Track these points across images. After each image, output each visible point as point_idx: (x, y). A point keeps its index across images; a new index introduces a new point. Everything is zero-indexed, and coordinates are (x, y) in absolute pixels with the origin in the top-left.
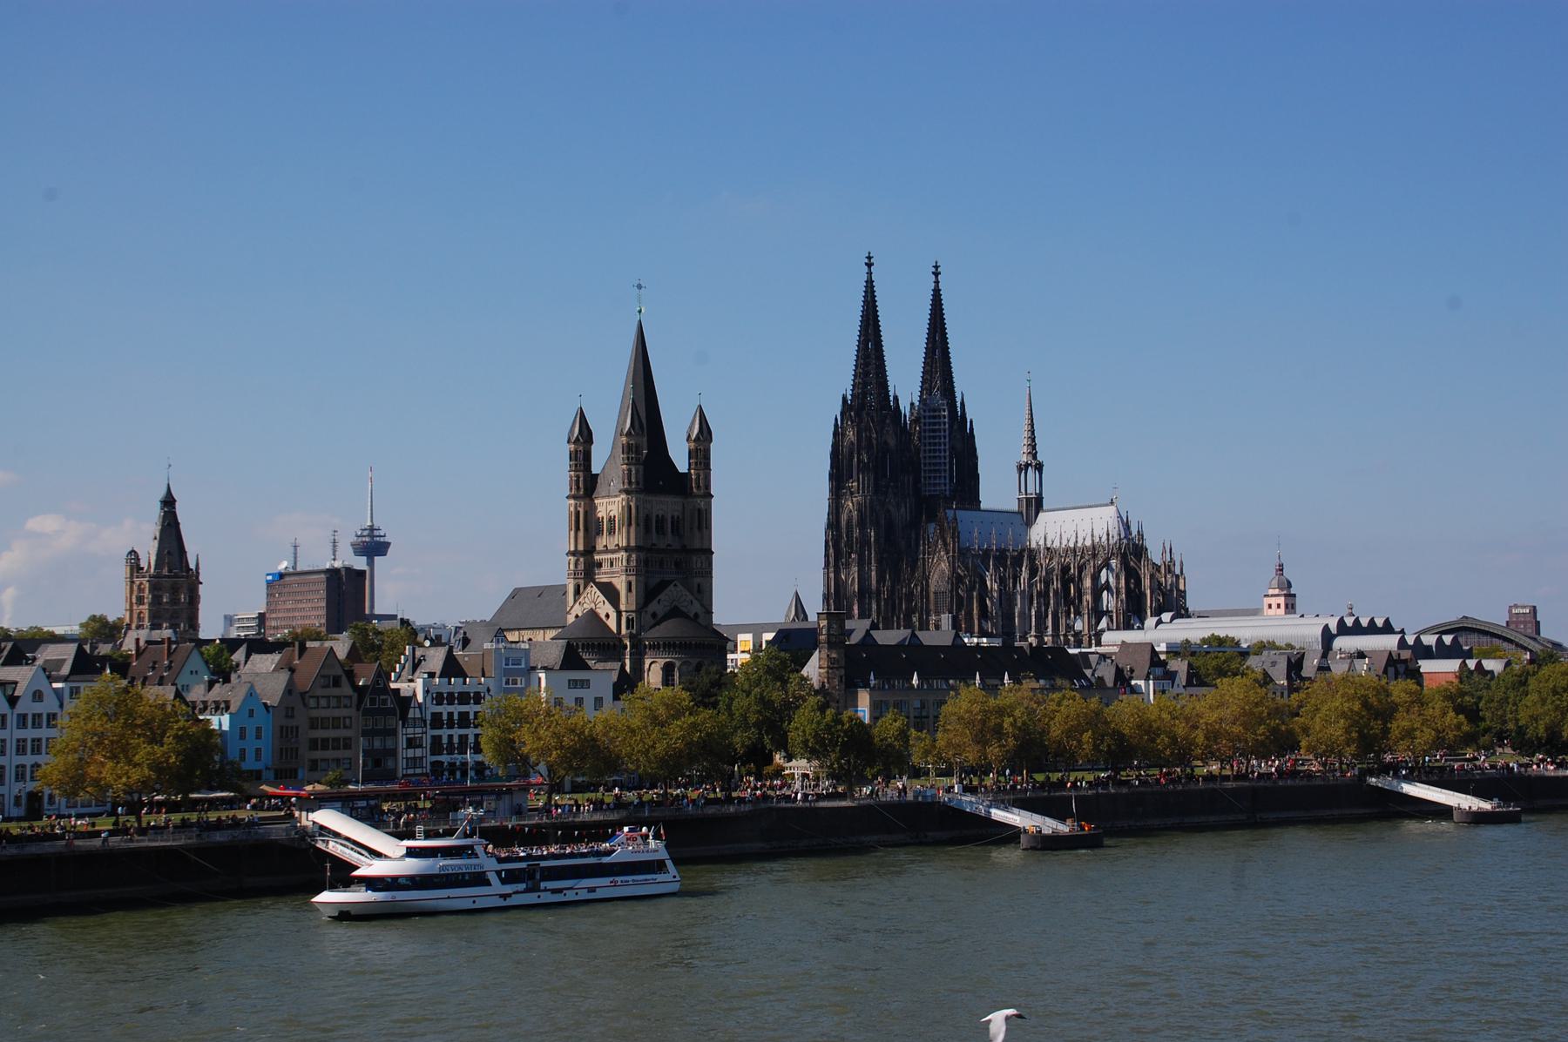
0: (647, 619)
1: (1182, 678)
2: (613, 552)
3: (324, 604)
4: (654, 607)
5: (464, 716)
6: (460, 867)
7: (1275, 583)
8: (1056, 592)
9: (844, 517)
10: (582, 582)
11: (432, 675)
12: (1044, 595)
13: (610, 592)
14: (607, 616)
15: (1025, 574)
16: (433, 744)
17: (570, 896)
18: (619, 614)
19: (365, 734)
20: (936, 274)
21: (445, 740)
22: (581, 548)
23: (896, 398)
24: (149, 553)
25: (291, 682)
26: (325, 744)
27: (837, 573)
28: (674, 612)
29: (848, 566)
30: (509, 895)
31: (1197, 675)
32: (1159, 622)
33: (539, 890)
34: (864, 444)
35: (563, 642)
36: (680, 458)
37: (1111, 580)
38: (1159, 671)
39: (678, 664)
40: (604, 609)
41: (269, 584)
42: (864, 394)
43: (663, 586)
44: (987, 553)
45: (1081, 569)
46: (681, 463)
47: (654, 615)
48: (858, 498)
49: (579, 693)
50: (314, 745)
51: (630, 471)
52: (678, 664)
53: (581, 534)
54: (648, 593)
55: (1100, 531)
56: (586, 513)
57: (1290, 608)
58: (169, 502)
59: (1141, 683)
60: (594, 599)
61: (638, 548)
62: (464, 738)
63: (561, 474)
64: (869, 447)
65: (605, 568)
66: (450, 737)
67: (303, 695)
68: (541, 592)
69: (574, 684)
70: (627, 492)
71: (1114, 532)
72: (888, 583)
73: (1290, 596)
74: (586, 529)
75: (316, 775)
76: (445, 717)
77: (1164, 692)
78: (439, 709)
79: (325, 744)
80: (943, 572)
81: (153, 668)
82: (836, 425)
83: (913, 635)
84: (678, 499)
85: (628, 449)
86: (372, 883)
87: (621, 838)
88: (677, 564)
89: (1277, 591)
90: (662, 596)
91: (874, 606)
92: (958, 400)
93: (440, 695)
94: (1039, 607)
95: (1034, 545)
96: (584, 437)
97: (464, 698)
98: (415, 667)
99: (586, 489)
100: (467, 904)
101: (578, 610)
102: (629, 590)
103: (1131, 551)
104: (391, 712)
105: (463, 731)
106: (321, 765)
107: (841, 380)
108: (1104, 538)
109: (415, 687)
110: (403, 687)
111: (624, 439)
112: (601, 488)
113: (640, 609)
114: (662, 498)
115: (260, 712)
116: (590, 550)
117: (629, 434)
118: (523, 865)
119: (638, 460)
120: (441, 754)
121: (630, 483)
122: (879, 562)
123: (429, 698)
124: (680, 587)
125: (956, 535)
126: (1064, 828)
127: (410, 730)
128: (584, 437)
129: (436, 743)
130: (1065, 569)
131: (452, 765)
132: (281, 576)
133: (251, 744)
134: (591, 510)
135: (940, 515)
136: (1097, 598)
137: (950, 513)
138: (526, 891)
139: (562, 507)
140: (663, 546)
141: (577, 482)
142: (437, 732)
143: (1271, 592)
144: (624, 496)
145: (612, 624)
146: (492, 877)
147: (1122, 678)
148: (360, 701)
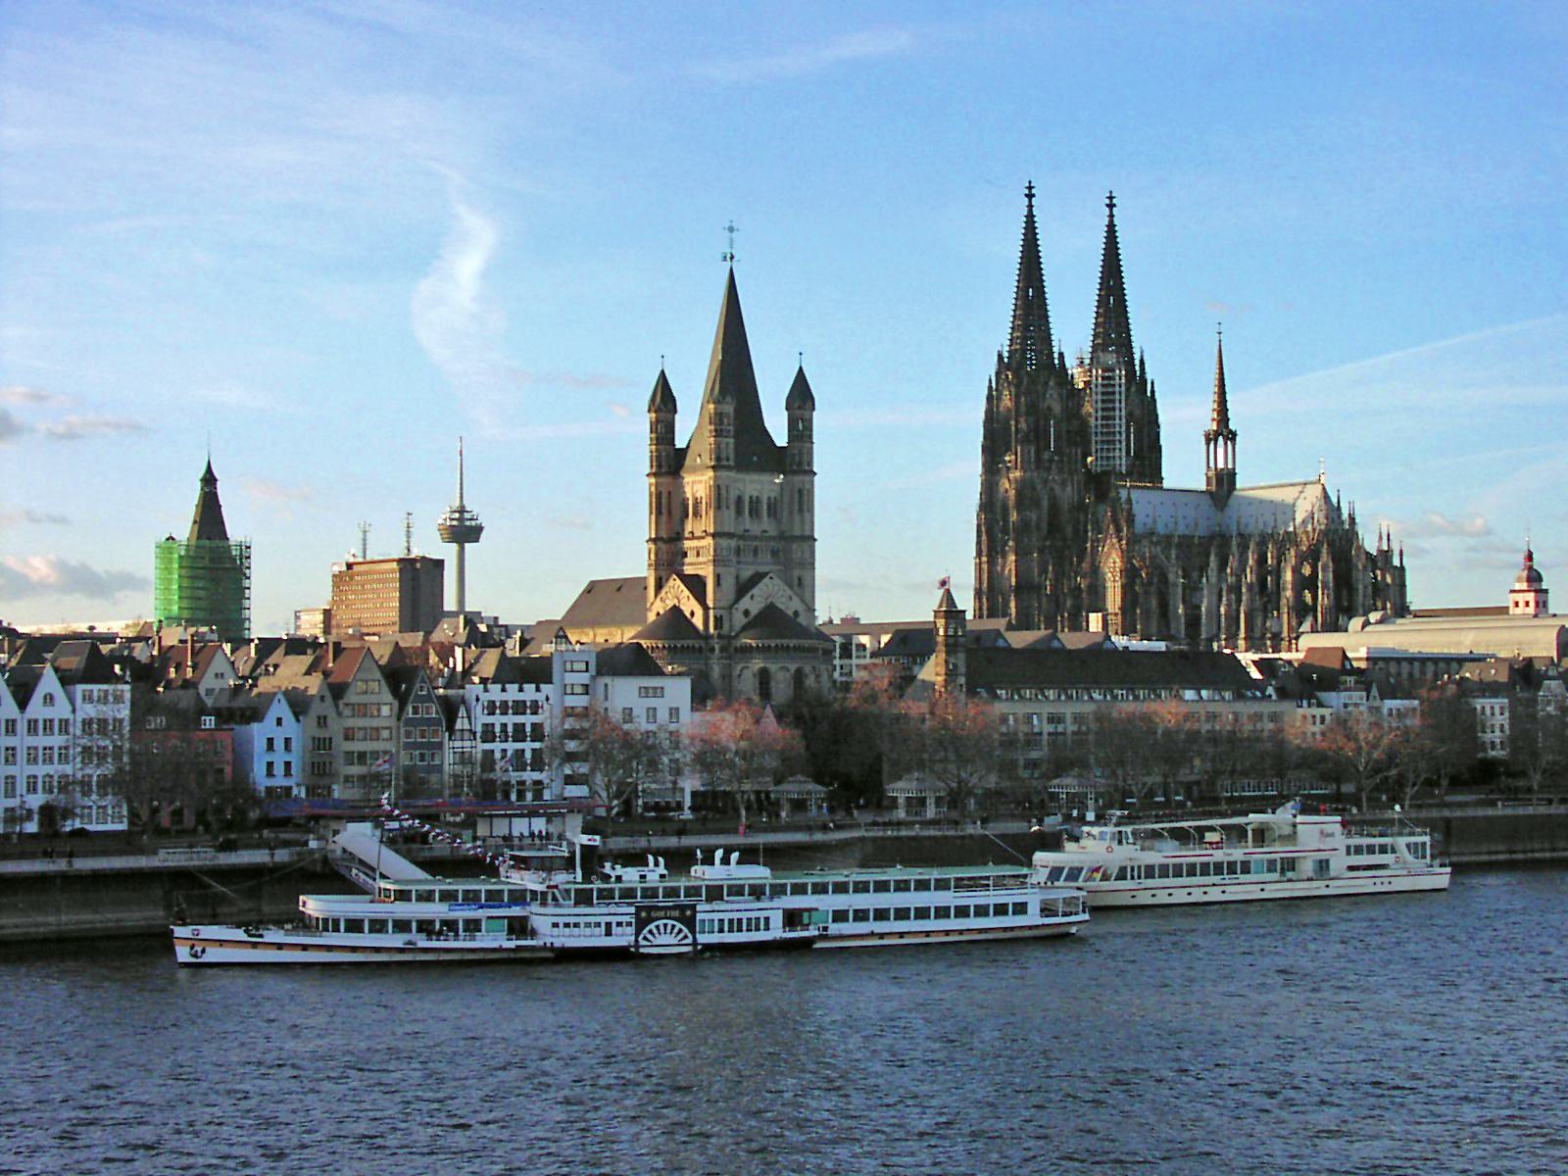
4: (745, 603)
5: (519, 728)
8: (1250, 587)
12: (1236, 589)
13: (696, 585)
14: (692, 614)
18: (706, 608)
23: (1061, 355)
27: (991, 563)
29: (1004, 556)
32: (1366, 623)
36: (777, 426)
40: (690, 605)
43: (757, 578)
46: (781, 439)
47: (746, 613)
49: (652, 702)
58: (209, 480)
60: (678, 594)
65: (687, 560)
68: (620, 585)
69: (645, 692)
74: (670, 513)
76: (497, 729)
78: (490, 719)
82: (990, 387)
88: (774, 553)
90: (755, 591)
92: (1137, 357)
94: (1229, 605)
96: (664, 401)
97: (520, 708)
99: (669, 466)
105: (519, 745)
107: (997, 333)
114: (755, 477)
124: (777, 581)
125: (1131, 520)
127: (458, 744)
133: (279, 757)
137: (1124, 494)
139: (639, 486)
142: (488, 746)
143: (1517, 586)
145: (698, 621)
148: (402, 709)
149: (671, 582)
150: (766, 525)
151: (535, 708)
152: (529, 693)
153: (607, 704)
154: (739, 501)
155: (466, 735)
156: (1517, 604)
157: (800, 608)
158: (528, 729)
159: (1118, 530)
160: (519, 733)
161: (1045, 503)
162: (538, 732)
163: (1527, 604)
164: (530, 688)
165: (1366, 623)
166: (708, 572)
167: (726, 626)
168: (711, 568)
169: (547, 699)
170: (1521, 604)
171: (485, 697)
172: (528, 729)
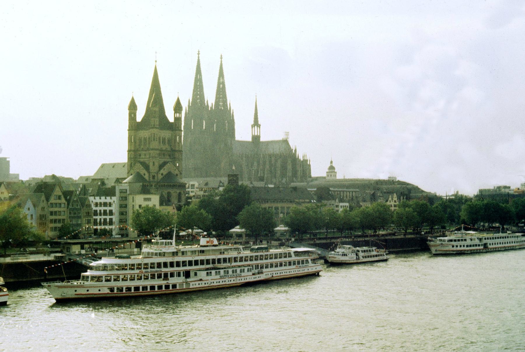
4: (162, 171)
5: (105, 211)
14: (145, 174)
16: (94, 223)
21: (98, 221)
43: (165, 163)
46: (171, 119)
47: (162, 174)
62: (105, 220)
66: (100, 219)
69: (145, 199)
76: (98, 212)
84: (171, 132)
88: (169, 156)
90: (165, 167)
97: (105, 204)
128: (133, 107)
140: (164, 149)
145: (146, 177)
148: (68, 204)
150: (166, 147)
151: (110, 205)
152: (108, 200)
153: (134, 203)
154: (159, 138)
157: (178, 173)
158: (108, 212)
160: (105, 213)
162: (111, 213)
164: (108, 198)
167: (156, 178)
171: (95, 201)
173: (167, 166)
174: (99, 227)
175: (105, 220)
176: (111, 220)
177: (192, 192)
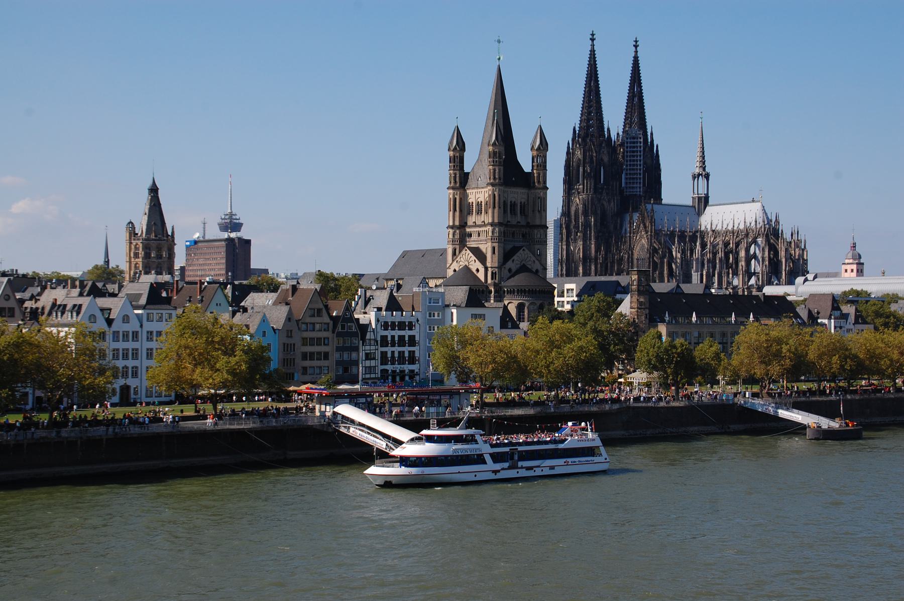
0: (505, 273)
1: (852, 318)
2: (480, 226)
3: (224, 261)
4: (509, 264)
5: (402, 338)
6: (466, 450)
7: (850, 255)
8: (721, 260)
9: (573, 209)
10: (457, 247)
11: (379, 309)
12: (712, 262)
13: (479, 254)
14: (478, 270)
15: (698, 247)
17: (538, 472)
18: (486, 269)
19: (339, 349)
20: (636, 46)
21: (389, 355)
22: (457, 223)
23: (608, 129)
24: (141, 225)
25: (290, 312)
26: (311, 356)
27: (568, 245)
28: (523, 269)
29: (575, 240)
30: (498, 471)
31: (861, 316)
32: (806, 280)
33: (517, 468)
34: (587, 160)
35: (467, 288)
37: (757, 252)
38: (837, 313)
39: (527, 304)
41: (187, 247)
42: (588, 127)
44: (672, 234)
45: (737, 244)
46: (527, 168)
47: (510, 270)
48: (583, 196)
50: (305, 356)
51: (495, 170)
52: (527, 304)
53: (457, 214)
54: (506, 256)
55: (750, 219)
56: (461, 199)
57: (860, 272)
58: (154, 190)
59: (826, 321)
60: (467, 258)
61: (500, 224)
62: (401, 354)
63: (444, 172)
64: (591, 162)
65: (473, 238)
66: (393, 352)
67: (298, 321)
68: (424, 253)
69: (475, 316)
70: (493, 185)
71: (760, 220)
72: (603, 253)
73: (860, 264)
74: (461, 211)
75: (307, 378)
76: (389, 339)
77: (841, 328)
78: (385, 333)
79: (311, 356)
80: (643, 245)
81: (190, 301)
82: (568, 147)
83: (678, 286)
85: (493, 155)
86: (404, 461)
87: (568, 431)
88: (523, 236)
89: (851, 261)
90: (515, 257)
91: (593, 267)
93: (386, 323)
94: (708, 269)
95: (703, 228)
97: (402, 326)
98: (367, 302)
99: (461, 183)
100: (470, 478)
101: (455, 266)
102: (494, 253)
103: (772, 233)
104: (354, 335)
106: (309, 371)
108: (753, 224)
109: (369, 317)
110: (363, 319)
111: (491, 148)
112: (471, 181)
113: (501, 267)
115: (270, 333)
116: (463, 225)
117: (494, 144)
118: (507, 449)
119: (500, 162)
120: (386, 364)
121: (495, 178)
122: (597, 238)
123: (379, 326)
125: (653, 221)
126: (835, 424)
127: (368, 348)
128: (460, 146)
129: (384, 359)
130: (726, 244)
131: (394, 372)
132: (196, 242)
134: (464, 197)
135: (643, 207)
136: (748, 264)
138: (510, 468)
139: (444, 195)
140: (514, 223)
141: (455, 177)
142: (384, 349)
143: (847, 261)
144: (490, 188)
146: (488, 458)
147: (813, 318)
148: (335, 327)
149: (464, 252)
151: (411, 326)
155: (372, 342)
156: (846, 271)
158: (407, 339)
159: (645, 227)
160: (401, 341)
161: (599, 212)
162: (412, 341)
163: (852, 271)
165: (806, 280)
166: (486, 248)
168: (489, 244)
169: (418, 321)
170: (849, 271)
172: (407, 339)
173: (518, 254)
174: (389, 367)
175: (401, 354)
176: (412, 353)
177: (568, 302)
